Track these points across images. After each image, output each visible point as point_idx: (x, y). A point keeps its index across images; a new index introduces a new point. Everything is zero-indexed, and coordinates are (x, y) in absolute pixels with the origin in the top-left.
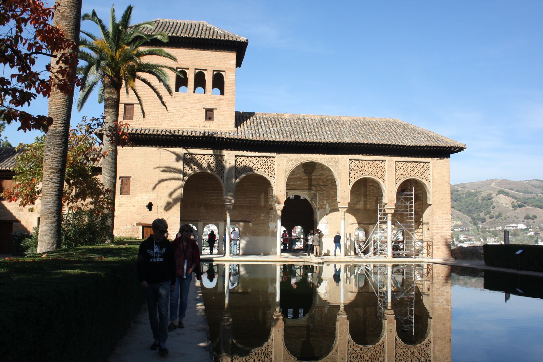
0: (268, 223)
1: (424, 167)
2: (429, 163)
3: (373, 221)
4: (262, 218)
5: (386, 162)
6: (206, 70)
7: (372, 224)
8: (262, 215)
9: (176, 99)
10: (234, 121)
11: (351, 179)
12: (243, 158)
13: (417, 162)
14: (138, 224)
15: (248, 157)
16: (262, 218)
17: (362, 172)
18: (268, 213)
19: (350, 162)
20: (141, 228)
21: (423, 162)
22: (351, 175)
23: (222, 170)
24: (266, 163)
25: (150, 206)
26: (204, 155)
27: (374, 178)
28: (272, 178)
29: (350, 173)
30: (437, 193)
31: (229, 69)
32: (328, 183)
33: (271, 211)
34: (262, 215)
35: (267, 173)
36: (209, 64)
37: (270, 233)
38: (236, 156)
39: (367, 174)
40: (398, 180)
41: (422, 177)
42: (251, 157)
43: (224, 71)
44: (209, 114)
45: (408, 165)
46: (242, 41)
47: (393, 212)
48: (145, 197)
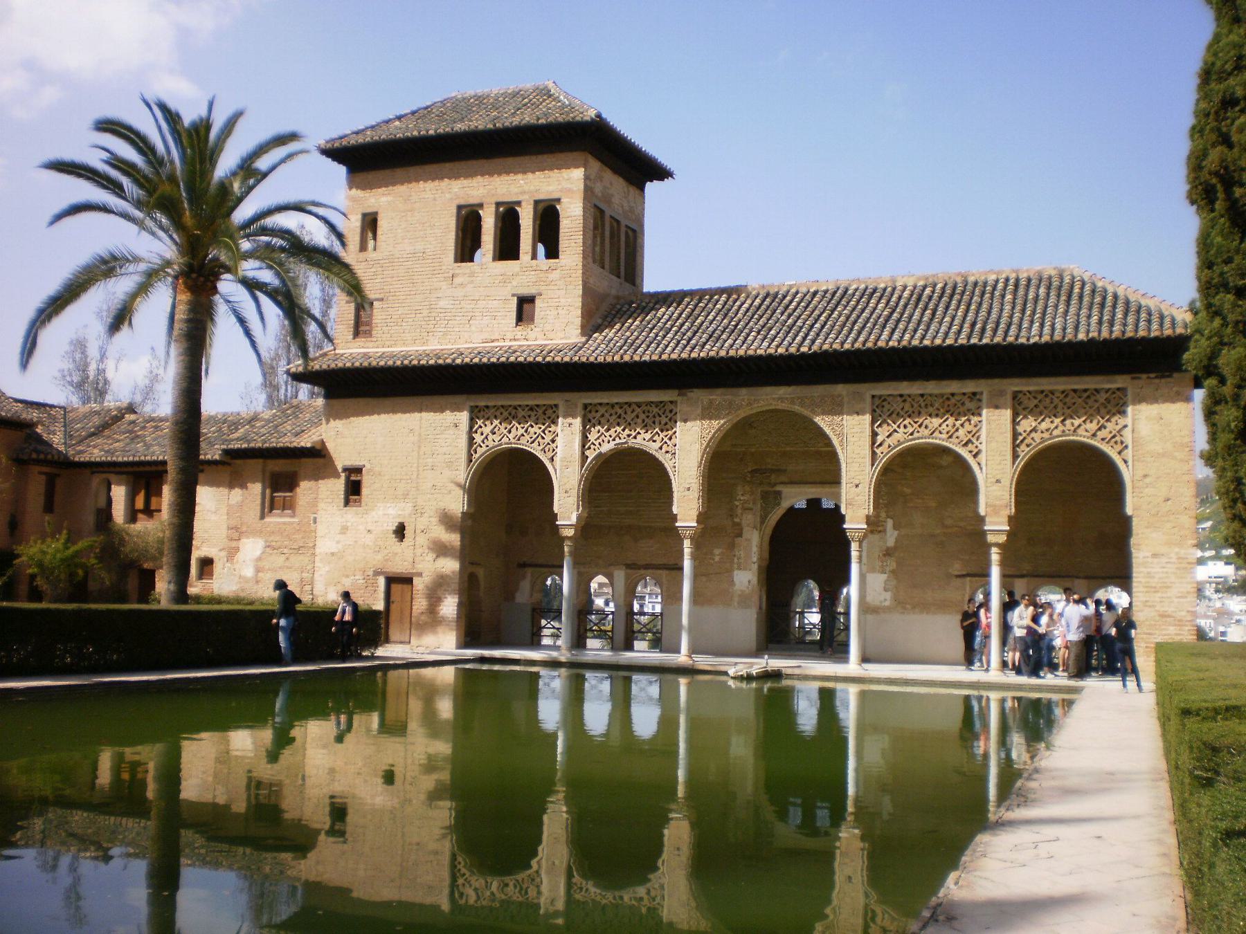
0: (730, 571)
1: (1109, 407)
2: (1122, 390)
3: (1027, 567)
4: (717, 558)
5: (985, 397)
6: (519, 203)
7: (1022, 576)
8: (717, 551)
9: (457, 280)
10: (578, 321)
11: (878, 451)
12: (602, 410)
13: (1085, 391)
14: (377, 573)
15: (613, 406)
16: (717, 558)
17: (910, 430)
18: (732, 546)
19: (877, 402)
20: (381, 581)
21: (1107, 391)
22: (879, 439)
23: (553, 441)
24: (657, 419)
25: (400, 532)
26: (515, 408)
27: (944, 443)
28: (669, 455)
29: (874, 435)
30: (1148, 480)
31: (569, 191)
32: (826, 466)
33: (738, 540)
34: (717, 551)
35: (658, 445)
36: (526, 188)
37: (736, 599)
38: (585, 406)
39: (927, 432)
40: (1023, 447)
41: (1100, 434)
42: (621, 405)
43: (558, 200)
44: (525, 307)
45: (1056, 401)
46: (588, 118)
47: (1002, 539)
48: (391, 511)
